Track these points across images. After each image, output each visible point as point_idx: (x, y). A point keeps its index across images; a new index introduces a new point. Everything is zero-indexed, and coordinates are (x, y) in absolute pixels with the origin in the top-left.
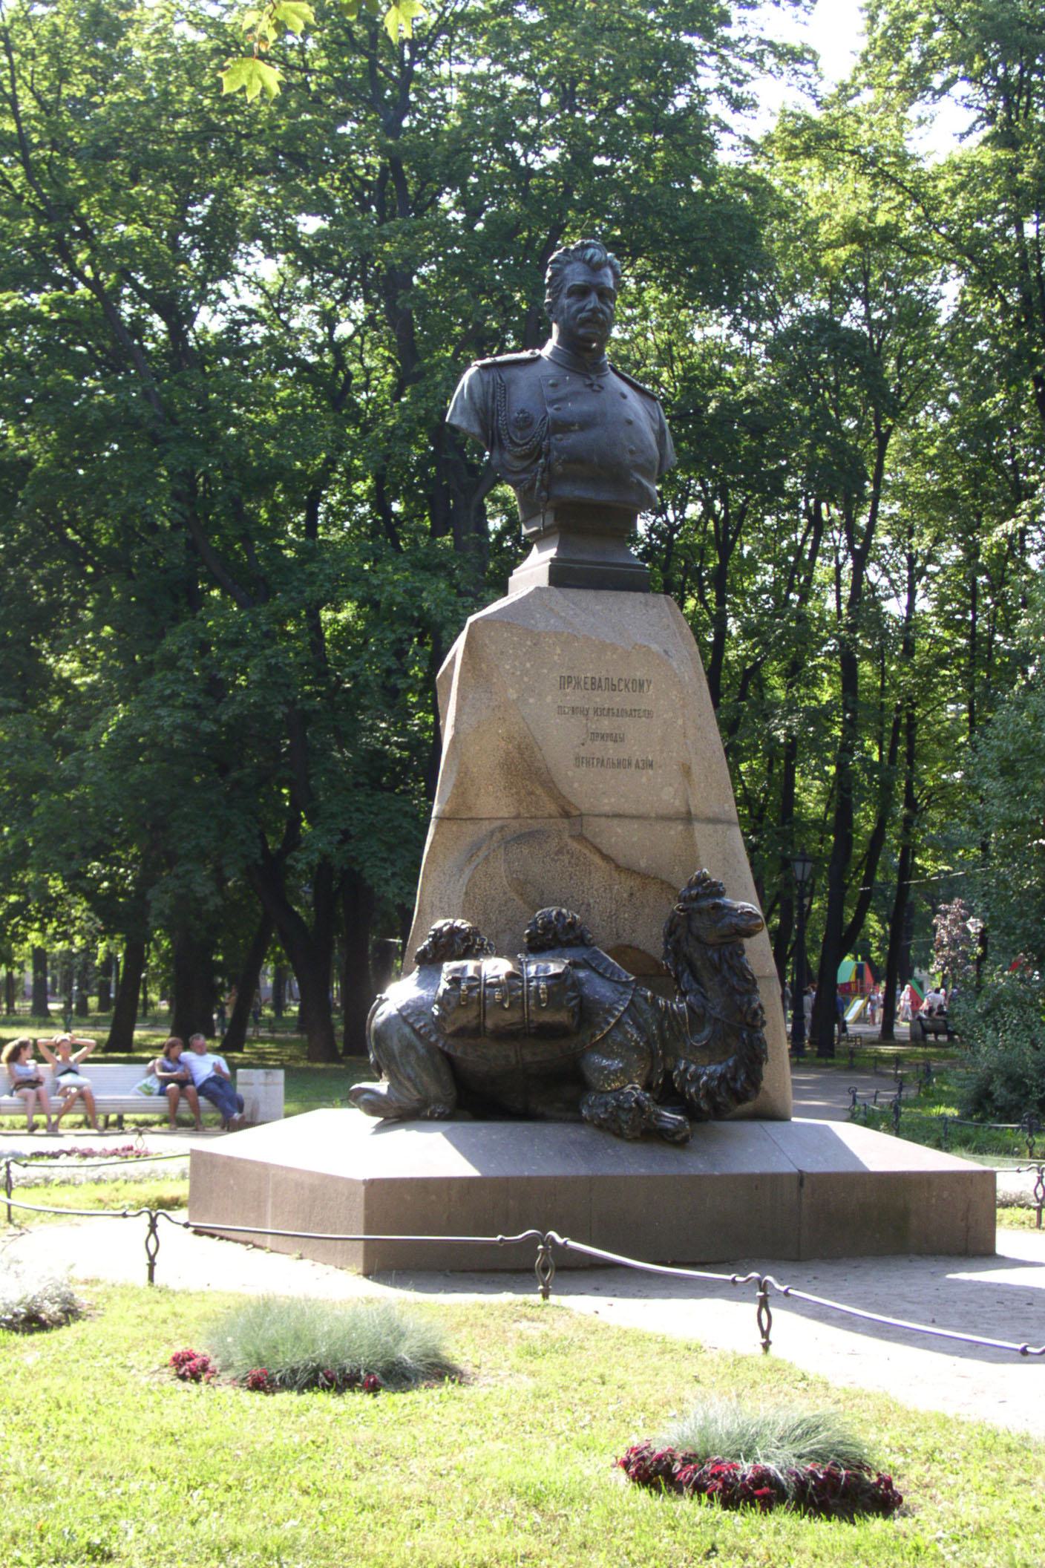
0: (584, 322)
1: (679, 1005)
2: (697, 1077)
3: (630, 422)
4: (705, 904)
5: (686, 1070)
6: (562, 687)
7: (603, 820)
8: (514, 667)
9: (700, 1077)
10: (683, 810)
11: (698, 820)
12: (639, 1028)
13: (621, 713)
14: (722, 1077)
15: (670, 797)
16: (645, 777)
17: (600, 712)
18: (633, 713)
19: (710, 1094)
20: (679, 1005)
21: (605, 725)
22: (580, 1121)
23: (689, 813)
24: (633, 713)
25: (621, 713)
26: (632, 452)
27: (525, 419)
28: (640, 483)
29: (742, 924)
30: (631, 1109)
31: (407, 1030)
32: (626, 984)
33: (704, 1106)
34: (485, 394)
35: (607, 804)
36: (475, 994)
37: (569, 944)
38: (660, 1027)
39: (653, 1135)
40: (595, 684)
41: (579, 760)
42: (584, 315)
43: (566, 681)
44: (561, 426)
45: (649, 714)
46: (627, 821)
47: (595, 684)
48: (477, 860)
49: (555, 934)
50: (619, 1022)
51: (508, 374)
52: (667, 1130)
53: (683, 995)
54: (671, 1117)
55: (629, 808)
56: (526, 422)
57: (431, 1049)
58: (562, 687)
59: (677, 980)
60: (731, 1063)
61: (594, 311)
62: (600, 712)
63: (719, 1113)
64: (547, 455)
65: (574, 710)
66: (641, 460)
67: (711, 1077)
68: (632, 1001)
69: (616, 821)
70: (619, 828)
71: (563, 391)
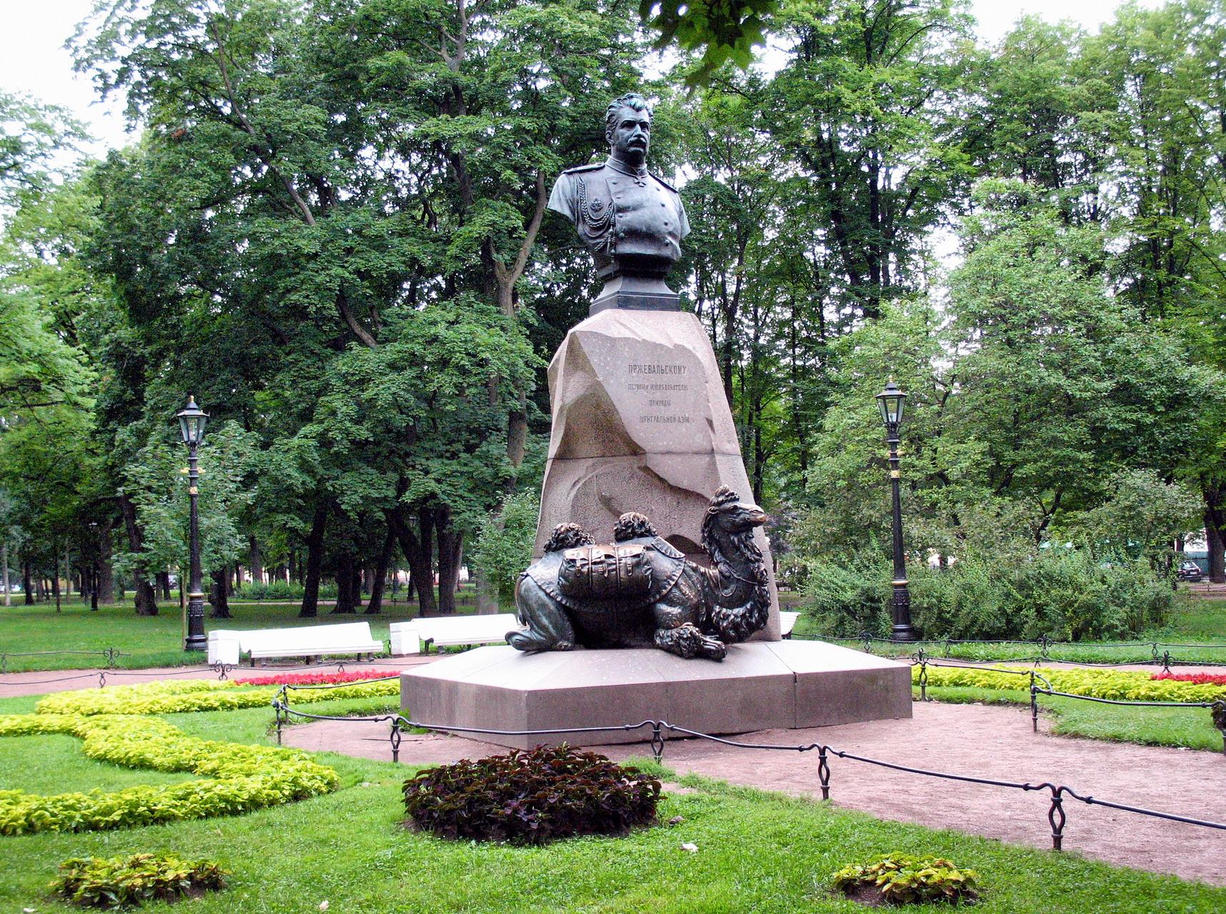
0: (632, 144)
1: (713, 572)
2: (726, 617)
4: (731, 505)
6: (630, 371)
10: (709, 448)
12: (690, 587)
13: (668, 387)
14: (743, 616)
15: (699, 441)
16: (683, 428)
17: (655, 387)
18: (675, 387)
19: (736, 626)
20: (713, 572)
21: (658, 395)
22: (654, 646)
24: (675, 387)
25: (668, 387)
29: (752, 518)
31: (542, 594)
33: (732, 633)
34: (572, 190)
35: (662, 445)
37: (642, 535)
38: (702, 586)
39: (698, 653)
40: (651, 370)
41: (643, 419)
42: (632, 139)
43: (633, 368)
44: (621, 210)
45: (685, 388)
46: (674, 456)
47: (651, 370)
50: (676, 585)
51: (585, 177)
53: (716, 564)
54: (711, 642)
55: (673, 447)
56: (597, 208)
57: (559, 604)
58: (630, 371)
59: (712, 555)
60: (748, 606)
61: (639, 136)
62: (655, 387)
63: (741, 638)
64: (614, 225)
65: (639, 387)
69: (667, 457)
70: (668, 460)
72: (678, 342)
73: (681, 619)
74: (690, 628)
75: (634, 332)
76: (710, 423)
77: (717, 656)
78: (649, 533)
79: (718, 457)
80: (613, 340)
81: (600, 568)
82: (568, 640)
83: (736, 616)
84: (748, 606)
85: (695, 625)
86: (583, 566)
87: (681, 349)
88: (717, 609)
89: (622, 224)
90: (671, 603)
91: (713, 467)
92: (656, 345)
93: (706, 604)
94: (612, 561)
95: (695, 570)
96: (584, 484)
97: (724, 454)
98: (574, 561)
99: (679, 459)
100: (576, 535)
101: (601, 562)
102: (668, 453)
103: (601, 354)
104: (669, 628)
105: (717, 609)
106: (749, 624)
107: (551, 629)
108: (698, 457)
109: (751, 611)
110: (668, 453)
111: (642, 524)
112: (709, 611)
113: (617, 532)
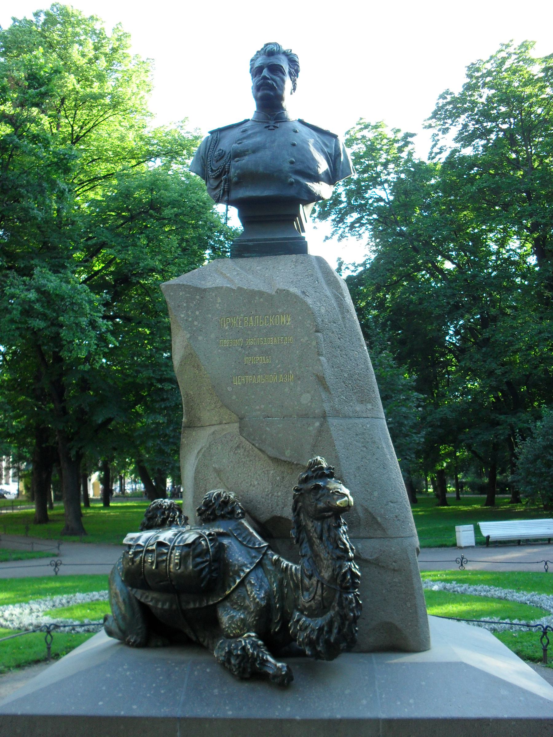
2: (304, 628)
3: (294, 145)
5: (298, 621)
8: (188, 316)
9: (306, 628)
14: (321, 629)
19: (312, 643)
26: (292, 163)
27: (219, 155)
28: (298, 182)
30: (238, 656)
32: (259, 550)
36: (138, 559)
37: (223, 517)
44: (238, 155)
48: (200, 456)
49: (214, 510)
64: (228, 172)
66: (299, 167)
71: (249, 132)
72: (282, 286)
75: (231, 281)
76: (321, 380)
78: (231, 515)
79: (333, 422)
80: (203, 291)
83: (313, 630)
87: (285, 294)
89: (237, 168)
92: (253, 294)
93: (282, 608)
96: (204, 455)
98: (130, 546)
101: (152, 551)
103: (188, 308)
104: (228, 637)
106: (327, 642)
111: (226, 502)
113: (201, 513)
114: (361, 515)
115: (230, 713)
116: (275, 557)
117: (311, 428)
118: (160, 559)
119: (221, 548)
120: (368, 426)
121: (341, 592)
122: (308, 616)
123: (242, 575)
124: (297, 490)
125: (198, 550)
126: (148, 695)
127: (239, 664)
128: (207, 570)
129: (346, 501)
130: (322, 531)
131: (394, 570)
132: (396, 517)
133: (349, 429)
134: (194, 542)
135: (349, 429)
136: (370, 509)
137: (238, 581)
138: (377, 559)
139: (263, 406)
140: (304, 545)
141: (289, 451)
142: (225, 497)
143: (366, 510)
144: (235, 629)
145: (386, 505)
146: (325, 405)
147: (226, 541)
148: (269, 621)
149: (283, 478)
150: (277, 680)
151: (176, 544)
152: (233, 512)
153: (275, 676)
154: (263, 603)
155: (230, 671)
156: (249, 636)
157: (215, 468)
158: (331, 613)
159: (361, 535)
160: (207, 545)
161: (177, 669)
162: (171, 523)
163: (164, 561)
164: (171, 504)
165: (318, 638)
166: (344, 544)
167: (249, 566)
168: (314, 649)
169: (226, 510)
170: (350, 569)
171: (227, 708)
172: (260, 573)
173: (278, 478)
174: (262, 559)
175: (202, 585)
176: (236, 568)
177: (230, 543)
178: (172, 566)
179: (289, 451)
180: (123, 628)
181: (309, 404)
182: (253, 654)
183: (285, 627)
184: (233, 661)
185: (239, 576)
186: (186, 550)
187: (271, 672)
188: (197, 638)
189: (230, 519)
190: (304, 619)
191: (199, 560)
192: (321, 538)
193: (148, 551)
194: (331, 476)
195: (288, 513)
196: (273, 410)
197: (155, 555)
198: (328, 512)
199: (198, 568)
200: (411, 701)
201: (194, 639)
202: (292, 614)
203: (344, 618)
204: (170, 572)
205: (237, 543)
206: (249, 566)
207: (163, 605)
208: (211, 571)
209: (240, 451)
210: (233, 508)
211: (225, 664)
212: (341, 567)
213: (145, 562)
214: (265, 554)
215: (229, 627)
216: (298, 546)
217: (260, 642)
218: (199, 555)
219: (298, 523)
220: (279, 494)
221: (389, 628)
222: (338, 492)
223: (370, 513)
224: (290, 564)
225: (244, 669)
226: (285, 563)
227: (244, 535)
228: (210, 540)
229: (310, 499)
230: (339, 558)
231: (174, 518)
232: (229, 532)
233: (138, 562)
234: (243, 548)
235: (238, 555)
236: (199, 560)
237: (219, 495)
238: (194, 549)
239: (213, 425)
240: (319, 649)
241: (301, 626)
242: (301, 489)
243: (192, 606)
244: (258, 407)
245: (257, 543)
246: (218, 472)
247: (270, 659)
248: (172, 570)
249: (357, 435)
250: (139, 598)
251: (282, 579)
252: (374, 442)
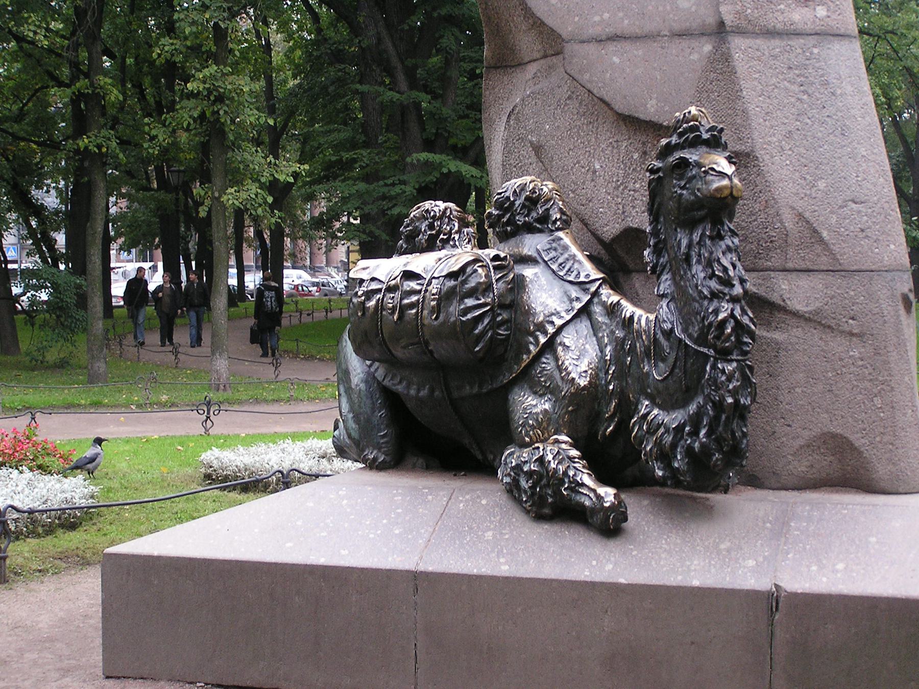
7: (592, 49)
9: (659, 426)
10: (711, 20)
11: (740, 32)
14: (679, 429)
23: (722, 24)
30: (530, 474)
35: (601, 19)
36: (372, 303)
37: (529, 229)
46: (627, 46)
52: (582, 505)
55: (626, 25)
60: (692, 408)
67: (667, 431)
68: (585, 311)
69: (611, 47)
70: (615, 56)
73: (545, 427)
74: (560, 453)
77: (609, 525)
78: (542, 224)
81: (390, 301)
82: (379, 449)
83: (667, 431)
84: (692, 408)
85: (575, 446)
86: (369, 294)
88: (644, 405)
90: (539, 391)
91: (721, 66)
94: (413, 285)
95: (612, 310)
97: (771, 33)
99: (638, 51)
100: (431, 226)
102: (615, 38)
104: (523, 445)
105: (644, 405)
106: (689, 451)
107: (352, 424)
108: (685, 43)
109: (695, 421)
110: (615, 38)
111: (533, 201)
112: (626, 409)
114: (789, 225)
115: (505, 568)
116: (615, 298)
117: (695, 57)
118: (406, 301)
119: (519, 284)
120: (816, 51)
121: (716, 359)
122: (661, 407)
123: (551, 330)
124: (652, 171)
125: (472, 283)
126: (372, 536)
127: (533, 488)
128: (486, 321)
129: (725, 187)
130: (690, 246)
131: (852, 334)
132: (862, 231)
133: (775, 57)
134: (463, 269)
135: (775, 57)
136: (807, 215)
137: (543, 340)
138: (817, 312)
139: (606, 16)
140: (664, 277)
141: (654, 102)
142: (533, 191)
143: (800, 216)
144: (533, 427)
145: (841, 207)
146: (723, 9)
147: (529, 272)
148: (595, 418)
149: (645, 153)
150: (597, 519)
151: (436, 275)
152: (544, 219)
153: (593, 511)
154: (583, 382)
155: (518, 501)
156: (557, 441)
157: (531, 142)
158: (701, 400)
159: (790, 265)
160: (487, 276)
161: (430, 497)
162: (445, 242)
163: (412, 305)
164: (446, 209)
165: (674, 446)
166: (725, 270)
167: (563, 314)
168: (668, 466)
169: (534, 214)
170: (732, 315)
171: (502, 560)
172: (583, 326)
173: (636, 156)
174: (589, 302)
175: (477, 349)
176: (541, 319)
177: (536, 274)
178: (425, 312)
179: (654, 102)
180: (355, 435)
181: (693, 9)
182: (556, 471)
183: (623, 427)
184: (524, 484)
185: (545, 333)
186: (452, 283)
187: (587, 503)
188: (483, 453)
189: (540, 231)
190: (656, 412)
191: (470, 302)
192: (688, 259)
193: (390, 289)
194: (715, 143)
195: (641, 220)
196: (626, 22)
197: (398, 295)
198: (698, 209)
199: (469, 316)
200: (840, 566)
201: (480, 457)
202: (638, 402)
203: (719, 406)
204: (423, 325)
205: (548, 274)
206: (563, 314)
207: (419, 390)
208: (494, 325)
209: (573, 105)
210: (548, 210)
211: (513, 490)
212: (716, 312)
213: (383, 309)
214: (596, 294)
215: (523, 425)
216: (655, 277)
217: (574, 453)
218: (472, 293)
219: (655, 233)
220: (638, 186)
221: (838, 445)
222: (713, 169)
223: (808, 222)
224: (638, 312)
225: (542, 498)
226: (628, 308)
227: (560, 260)
228: (495, 268)
229: (676, 188)
230: (714, 295)
231: (450, 233)
232: (535, 255)
233: (372, 310)
234: (557, 283)
235: (546, 297)
236: (470, 302)
237: (523, 187)
238: (464, 282)
239: (535, 60)
240: (676, 465)
241: (649, 424)
242: (659, 170)
243: (467, 390)
244: (597, 18)
245: (582, 274)
246: (538, 149)
247: (587, 480)
248: (426, 322)
249: (790, 68)
250: (380, 379)
251: (624, 339)
252: (826, 84)
